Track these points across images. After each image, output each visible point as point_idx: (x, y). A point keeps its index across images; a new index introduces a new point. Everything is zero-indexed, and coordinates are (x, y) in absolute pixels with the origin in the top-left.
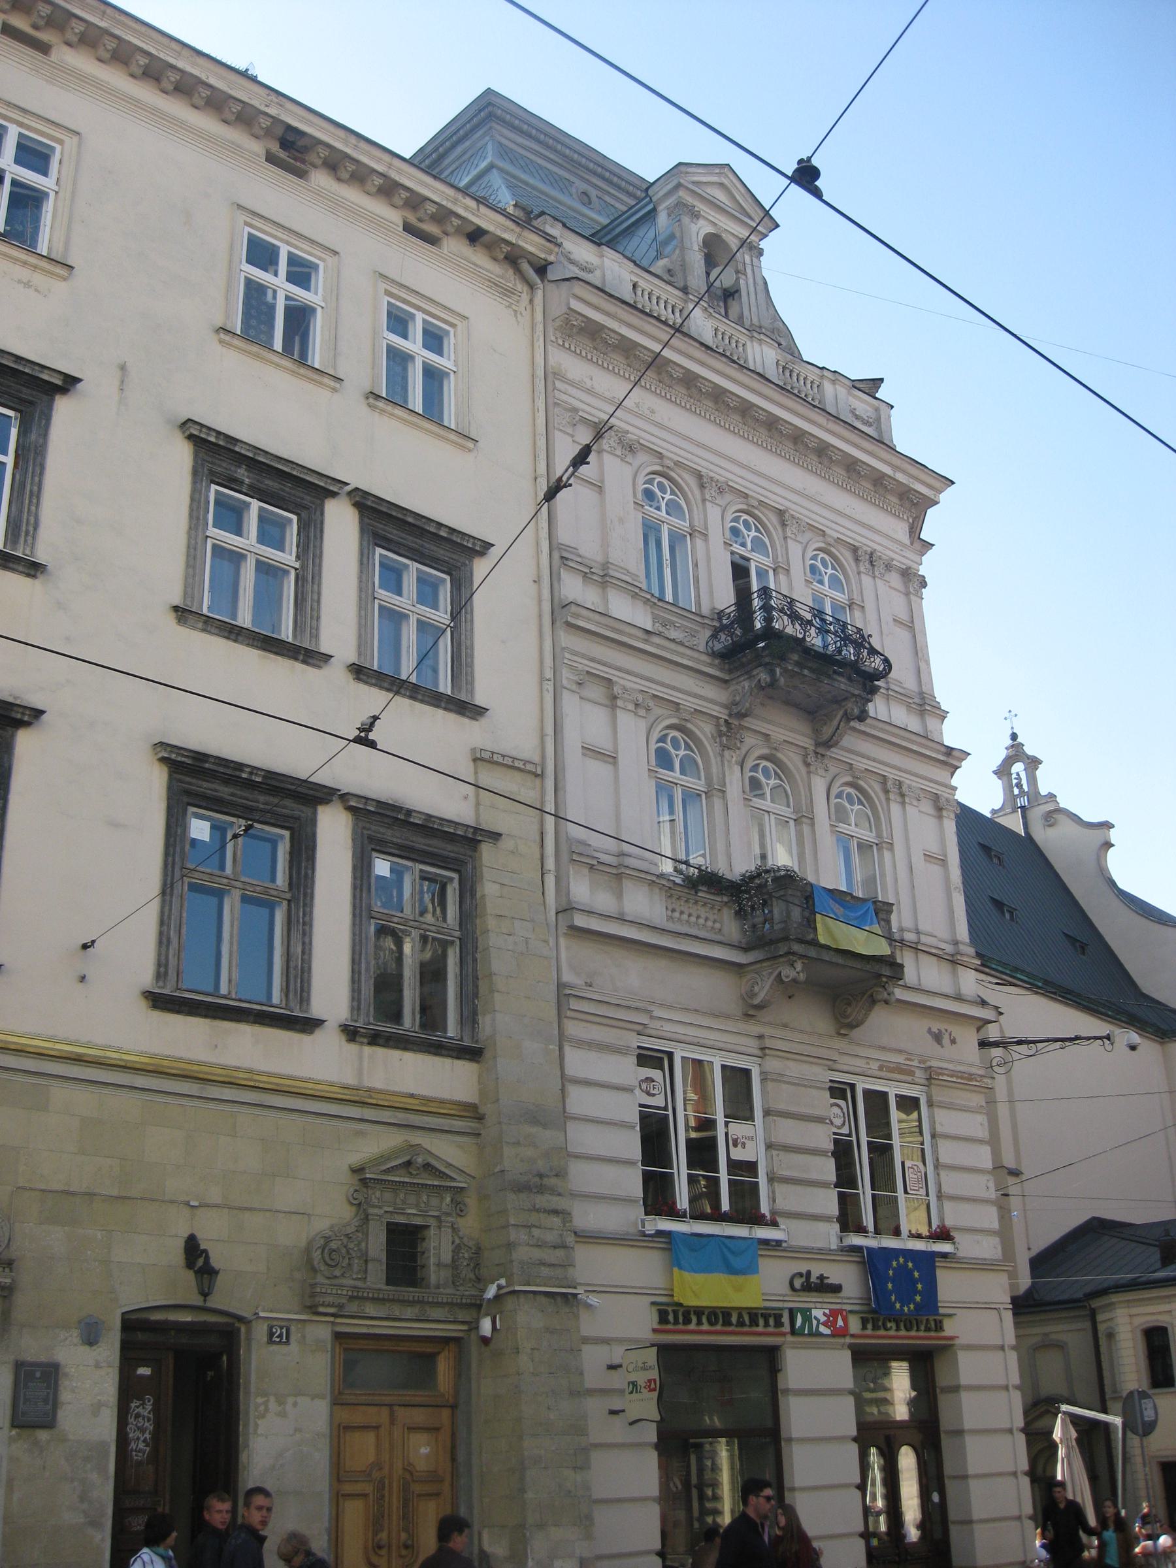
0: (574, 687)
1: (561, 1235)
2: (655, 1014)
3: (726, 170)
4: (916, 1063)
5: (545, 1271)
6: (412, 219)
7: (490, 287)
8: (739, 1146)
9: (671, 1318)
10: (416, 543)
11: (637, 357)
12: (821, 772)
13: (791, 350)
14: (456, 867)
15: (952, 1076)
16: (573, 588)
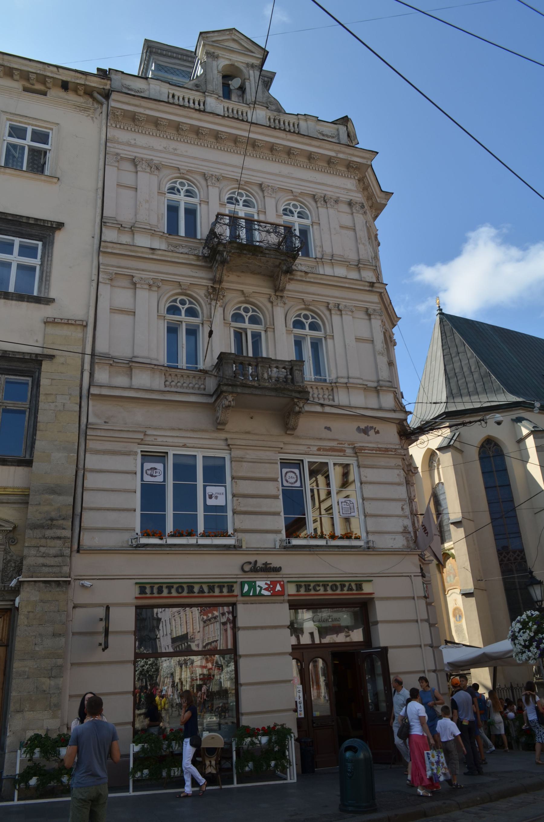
0: (108, 282)
1: (61, 550)
2: (147, 433)
3: (234, 31)
4: (346, 446)
5: (46, 570)
6: (28, 85)
7: (76, 108)
8: (213, 498)
9: (148, 590)
10: (17, 229)
11: (161, 124)
12: (282, 305)
13: (280, 110)
14: (29, 375)
15: (372, 450)
16: (110, 235)
